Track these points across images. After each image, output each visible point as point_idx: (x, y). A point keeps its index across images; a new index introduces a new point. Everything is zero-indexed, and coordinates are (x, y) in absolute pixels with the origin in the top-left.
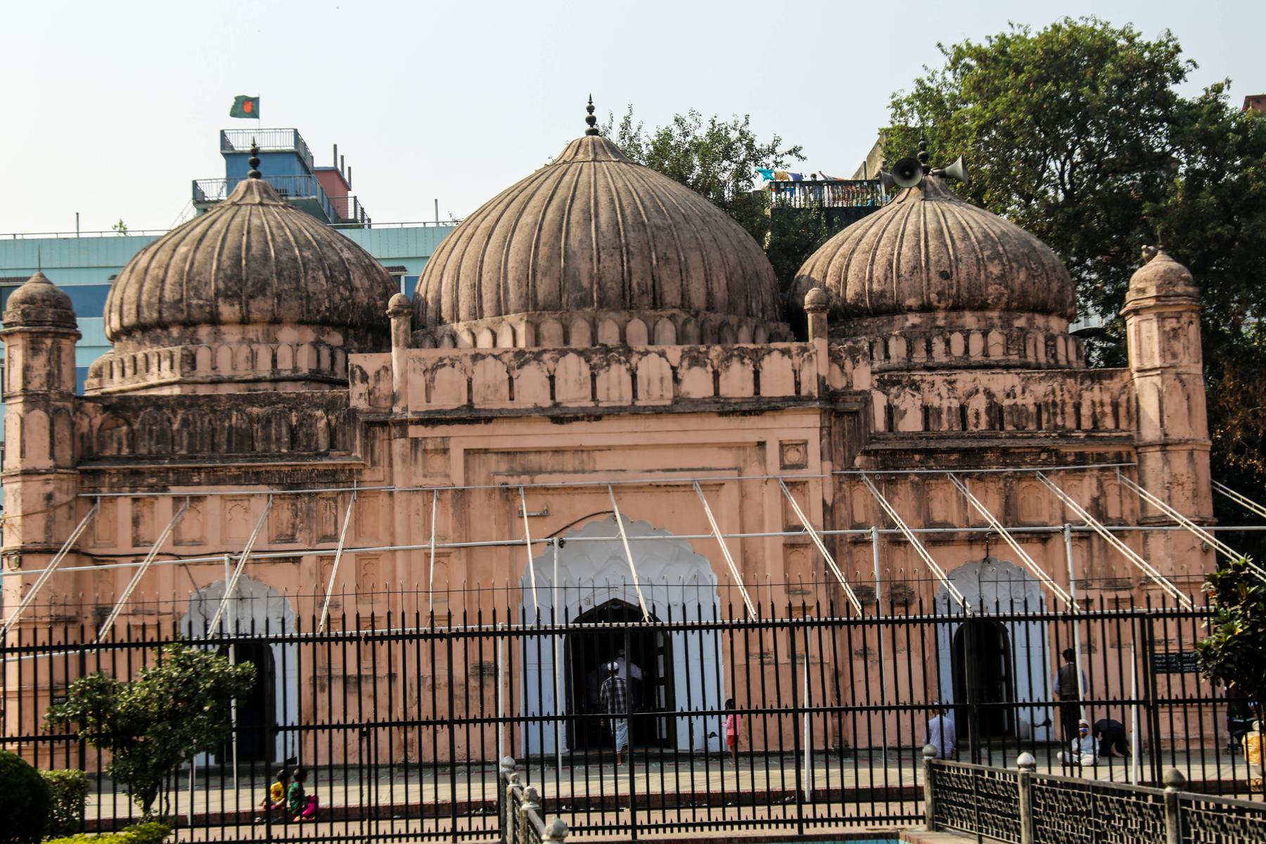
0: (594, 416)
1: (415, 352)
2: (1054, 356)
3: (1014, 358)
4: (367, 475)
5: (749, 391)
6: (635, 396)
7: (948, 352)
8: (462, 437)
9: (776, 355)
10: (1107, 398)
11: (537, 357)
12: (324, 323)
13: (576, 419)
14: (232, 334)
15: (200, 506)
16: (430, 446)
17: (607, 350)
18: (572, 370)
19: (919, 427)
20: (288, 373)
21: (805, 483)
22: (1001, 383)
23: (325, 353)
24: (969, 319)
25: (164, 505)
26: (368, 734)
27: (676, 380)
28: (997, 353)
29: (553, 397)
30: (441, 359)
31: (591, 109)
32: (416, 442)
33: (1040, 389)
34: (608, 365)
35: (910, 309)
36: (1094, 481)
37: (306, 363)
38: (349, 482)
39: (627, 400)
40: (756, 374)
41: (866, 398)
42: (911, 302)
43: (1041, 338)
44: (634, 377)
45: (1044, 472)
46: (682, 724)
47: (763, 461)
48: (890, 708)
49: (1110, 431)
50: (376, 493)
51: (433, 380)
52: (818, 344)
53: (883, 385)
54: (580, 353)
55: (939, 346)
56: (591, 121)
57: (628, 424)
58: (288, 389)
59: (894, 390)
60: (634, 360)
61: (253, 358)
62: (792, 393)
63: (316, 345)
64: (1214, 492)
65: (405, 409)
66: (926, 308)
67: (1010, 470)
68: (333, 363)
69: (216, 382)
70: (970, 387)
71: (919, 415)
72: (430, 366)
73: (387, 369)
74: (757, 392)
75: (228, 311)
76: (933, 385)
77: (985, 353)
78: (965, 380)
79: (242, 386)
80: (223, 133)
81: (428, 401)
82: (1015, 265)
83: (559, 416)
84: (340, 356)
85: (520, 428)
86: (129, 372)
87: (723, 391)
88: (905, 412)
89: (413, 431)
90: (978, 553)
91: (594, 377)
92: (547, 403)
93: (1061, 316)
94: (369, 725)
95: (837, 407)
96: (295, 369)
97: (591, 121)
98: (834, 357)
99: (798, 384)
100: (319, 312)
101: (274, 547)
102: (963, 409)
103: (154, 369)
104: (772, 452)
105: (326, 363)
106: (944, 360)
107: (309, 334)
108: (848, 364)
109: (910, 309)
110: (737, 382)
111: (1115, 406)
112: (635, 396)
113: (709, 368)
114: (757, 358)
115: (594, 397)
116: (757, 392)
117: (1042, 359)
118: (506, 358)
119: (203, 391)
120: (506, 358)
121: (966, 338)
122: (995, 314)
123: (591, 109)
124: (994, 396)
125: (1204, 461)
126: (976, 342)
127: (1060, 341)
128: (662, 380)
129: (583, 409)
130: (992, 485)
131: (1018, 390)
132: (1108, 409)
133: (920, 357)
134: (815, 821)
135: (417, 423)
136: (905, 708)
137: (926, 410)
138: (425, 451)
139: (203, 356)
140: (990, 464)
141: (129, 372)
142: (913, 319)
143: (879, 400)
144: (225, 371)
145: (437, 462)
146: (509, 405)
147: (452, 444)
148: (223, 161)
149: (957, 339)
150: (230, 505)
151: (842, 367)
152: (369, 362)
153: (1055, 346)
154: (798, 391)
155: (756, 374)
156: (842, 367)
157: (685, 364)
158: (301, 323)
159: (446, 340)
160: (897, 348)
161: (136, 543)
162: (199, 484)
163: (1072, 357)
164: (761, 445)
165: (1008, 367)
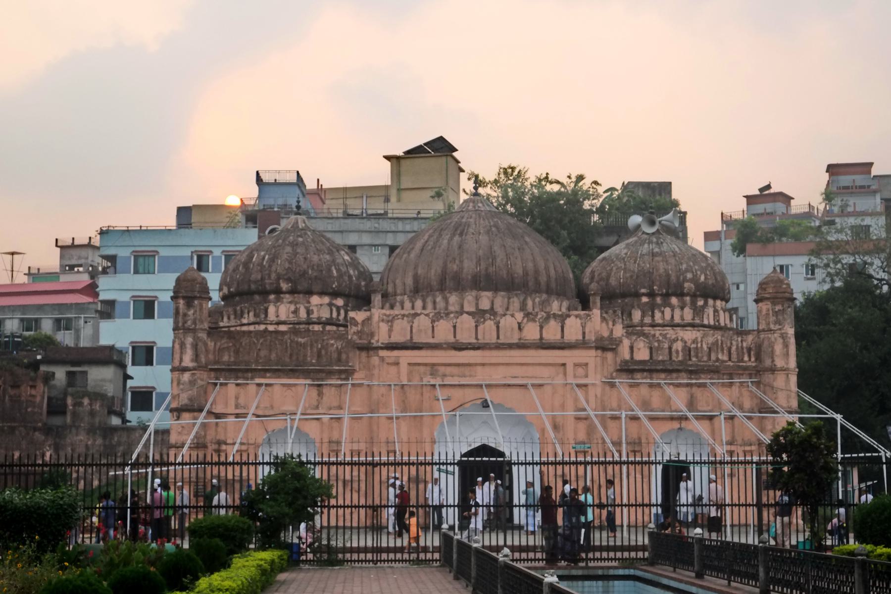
1: (384, 311)
2: (718, 321)
3: (697, 321)
4: (356, 375)
5: (559, 336)
6: (498, 338)
7: (663, 318)
8: (406, 356)
9: (573, 318)
11: (447, 314)
12: (335, 294)
13: (467, 349)
14: (287, 297)
15: (269, 389)
16: (391, 360)
17: (484, 312)
18: (467, 322)
19: (647, 358)
20: (315, 320)
21: (586, 386)
22: (689, 335)
23: (334, 309)
24: (674, 300)
25: (252, 388)
26: (377, 511)
27: (520, 329)
29: (455, 337)
30: (397, 315)
32: (382, 359)
33: (711, 340)
34: (485, 320)
35: (644, 294)
36: (737, 389)
37: (325, 314)
38: (347, 379)
39: (494, 340)
41: (621, 341)
42: (643, 291)
43: (710, 311)
44: (498, 327)
45: (711, 383)
46: (516, 510)
47: (565, 374)
48: (632, 505)
49: (745, 362)
50: (361, 385)
51: (392, 326)
52: (596, 312)
53: (629, 335)
54: (468, 313)
55: (658, 315)
57: (495, 353)
58: (317, 328)
59: (634, 338)
60: (498, 319)
61: (296, 312)
62: (581, 338)
63: (330, 305)
64: (799, 396)
65: (378, 341)
66: (651, 295)
67: (694, 381)
68: (339, 314)
69: (278, 323)
70: (674, 337)
71: (647, 352)
72: (391, 318)
73: (369, 319)
74: (563, 337)
75: (284, 286)
76: (654, 335)
77: (682, 318)
78: (670, 333)
79: (291, 326)
80: (258, 173)
81: (390, 337)
82: (699, 273)
83: (459, 347)
84: (342, 312)
86: (232, 317)
87: (544, 335)
88: (639, 349)
89: (383, 353)
90: (676, 425)
91: (476, 326)
92: (451, 339)
93: (722, 300)
94: (377, 506)
95: (606, 346)
96: (319, 318)
98: (603, 319)
99: (584, 333)
100: (332, 288)
101: (309, 411)
102: (670, 348)
103: (246, 316)
104: (570, 368)
105: (335, 315)
106: (660, 322)
107: (326, 300)
108: (611, 323)
109: (644, 294)
110: (552, 332)
112: (498, 338)
113: (538, 323)
114: (562, 318)
115: (477, 338)
116: (563, 337)
117: (712, 323)
118: (431, 315)
119: (271, 328)
120: (431, 315)
121: (673, 311)
122: (688, 299)
124: (686, 342)
125: (794, 379)
126: (677, 313)
127: (721, 313)
128: (512, 329)
129: (470, 344)
130: (685, 389)
131: (699, 340)
132: (745, 350)
133: (648, 320)
134: (594, 559)
135: (382, 348)
136: (640, 505)
137: (651, 349)
138: (388, 364)
139: (272, 310)
140: (683, 379)
141: (232, 317)
142: (645, 299)
143: (626, 342)
144: (283, 317)
145: (393, 369)
146: (431, 341)
147: (401, 361)
148: (256, 188)
149: (668, 311)
150: (285, 389)
151: (607, 324)
152: (359, 316)
153: (718, 316)
154: (584, 337)
156: (607, 324)
157: (526, 320)
158: (321, 294)
159: (398, 304)
160: (637, 315)
161: (237, 406)
162: (269, 378)
163: (728, 322)
164: (564, 365)
165: (693, 326)
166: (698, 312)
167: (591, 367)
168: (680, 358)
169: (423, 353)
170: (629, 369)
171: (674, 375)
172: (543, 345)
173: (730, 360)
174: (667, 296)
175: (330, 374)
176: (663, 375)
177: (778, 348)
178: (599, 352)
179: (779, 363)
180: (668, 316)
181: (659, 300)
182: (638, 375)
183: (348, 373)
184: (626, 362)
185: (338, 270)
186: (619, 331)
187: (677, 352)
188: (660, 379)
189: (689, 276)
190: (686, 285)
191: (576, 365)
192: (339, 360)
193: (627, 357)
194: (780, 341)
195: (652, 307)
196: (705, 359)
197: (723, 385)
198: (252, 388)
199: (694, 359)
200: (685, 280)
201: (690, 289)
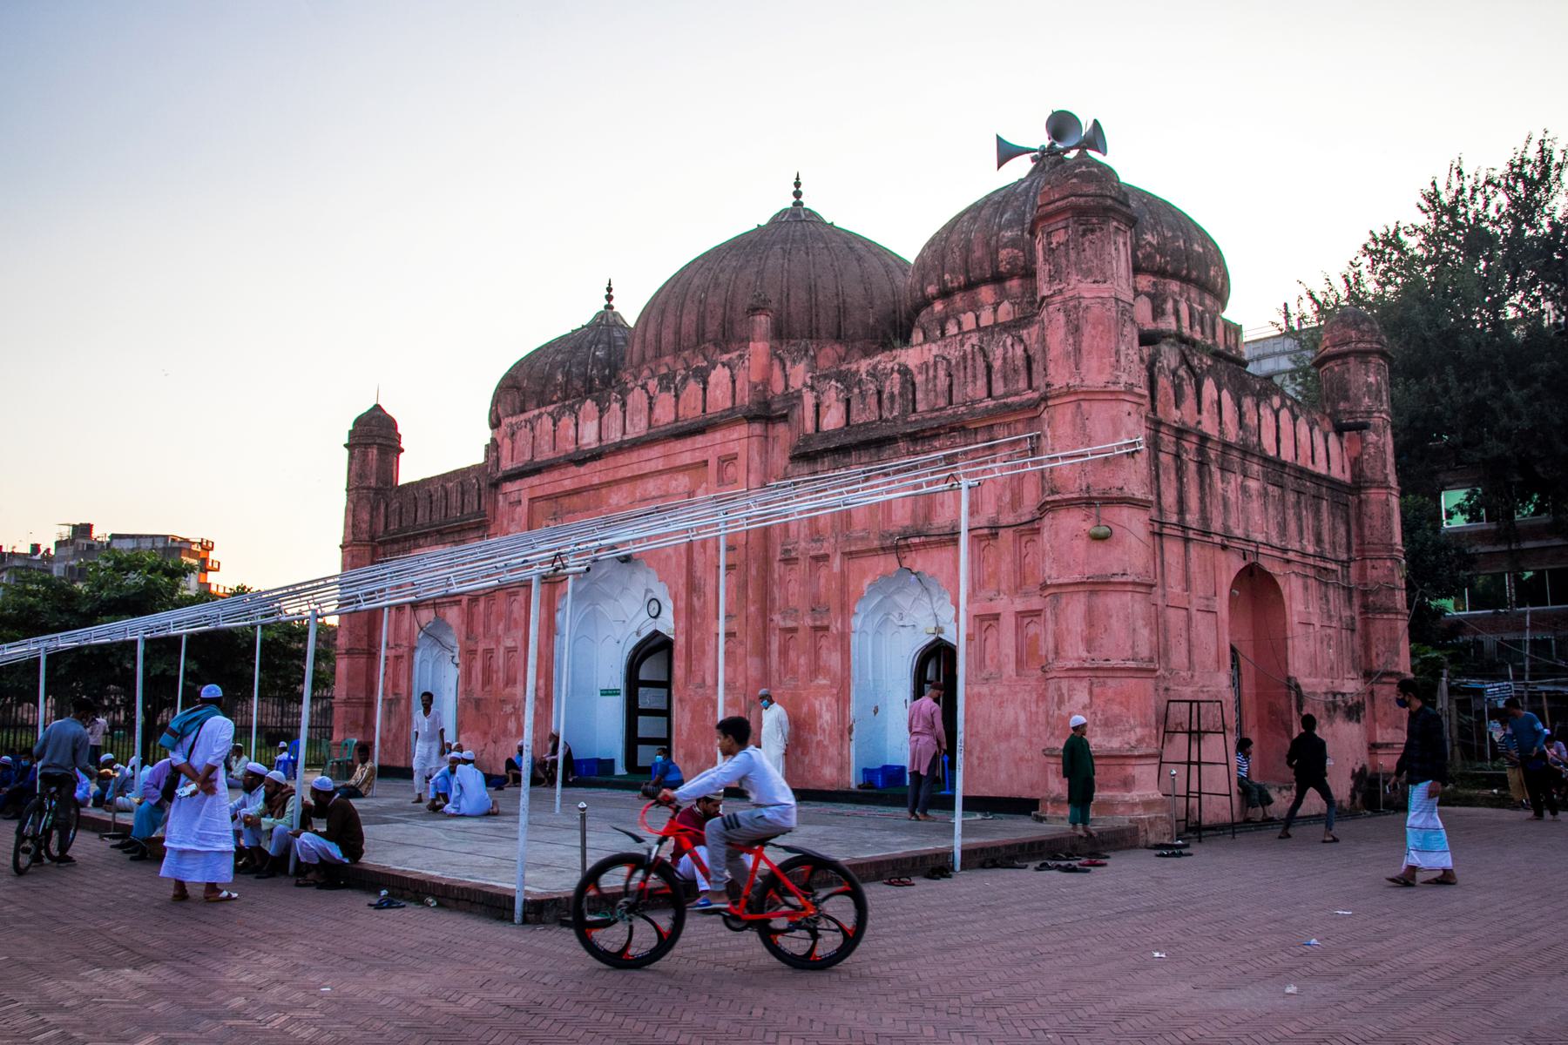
0: (596, 456)
10: (1019, 350)
31: (797, 185)
40: (704, 389)
56: (797, 194)
83: (582, 459)
92: (571, 448)
95: (766, 413)
97: (797, 194)
102: (880, 393)
115: (600, 439)
123: (797, 185)
143: (809, 399)
155: (704, 389)
168: (895, 413)
171: (887, 453)
173: (990, 395)
178: (757, 428)
186: (799, 374)
187: (892, 395)
190: (1004, 254)
199: (921, 407)
201: (1012, 261)
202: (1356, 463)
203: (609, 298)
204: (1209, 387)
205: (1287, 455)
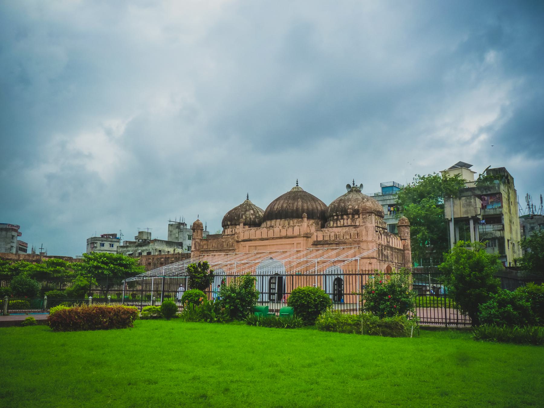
0: (267, 239)
3: (353, 224)
4: (237, 251)
24: (345, 217)
25: (211, 256)
28: (349, 223)
33: (344, 231)
55: (338, 222)
56: (297, 184)
61: (232, 231)
66: (337, 215)
75: (229, 223)
83: (262, 239)
85: (257, 242)
89: (242, 243)
92: (260, 237)
95: (307, 236)
97: (297, 184)
104: (295, 244)
111: (358, 234)
114: (293, 227)
142: (335, 217)
143: (315, 234)
160: (332, 223)
166: (353, 219)
167: (302, 244)
169: (253, 242)
170: (316, 244)
172: (287, 237)
174: (342, 215)
175: (230, 250)
176: (327, 246)
177: (364, 233)
178: (305, 238)
179: (364, 238)
180: (342, 223)
181: (340, 217)
182: (319, 246)
183: (234, 250)
184: (315, 241)
185: (246, 217)
188: (326, 247)
189: (350, 207)
190: (349, 210)
191: (297, 244)
192: (232, 246)
193: (316, 240)
194: (365, 229)
195: (337, 219)
196: (342, 238)
197: (348, 248)
198: (211, 256)
200: (348, 209)
202: (404, 246)
203: (248, 197)
204: (383, 236)
205: (393, 246)
